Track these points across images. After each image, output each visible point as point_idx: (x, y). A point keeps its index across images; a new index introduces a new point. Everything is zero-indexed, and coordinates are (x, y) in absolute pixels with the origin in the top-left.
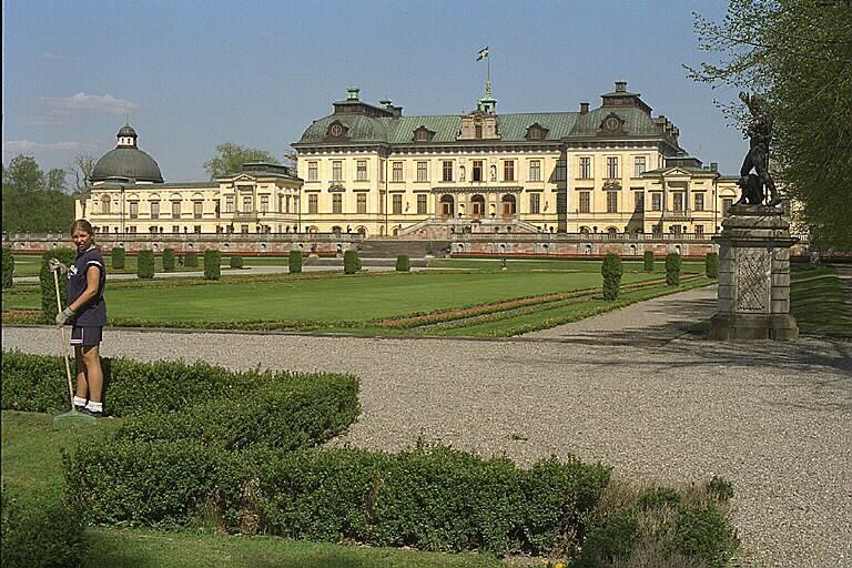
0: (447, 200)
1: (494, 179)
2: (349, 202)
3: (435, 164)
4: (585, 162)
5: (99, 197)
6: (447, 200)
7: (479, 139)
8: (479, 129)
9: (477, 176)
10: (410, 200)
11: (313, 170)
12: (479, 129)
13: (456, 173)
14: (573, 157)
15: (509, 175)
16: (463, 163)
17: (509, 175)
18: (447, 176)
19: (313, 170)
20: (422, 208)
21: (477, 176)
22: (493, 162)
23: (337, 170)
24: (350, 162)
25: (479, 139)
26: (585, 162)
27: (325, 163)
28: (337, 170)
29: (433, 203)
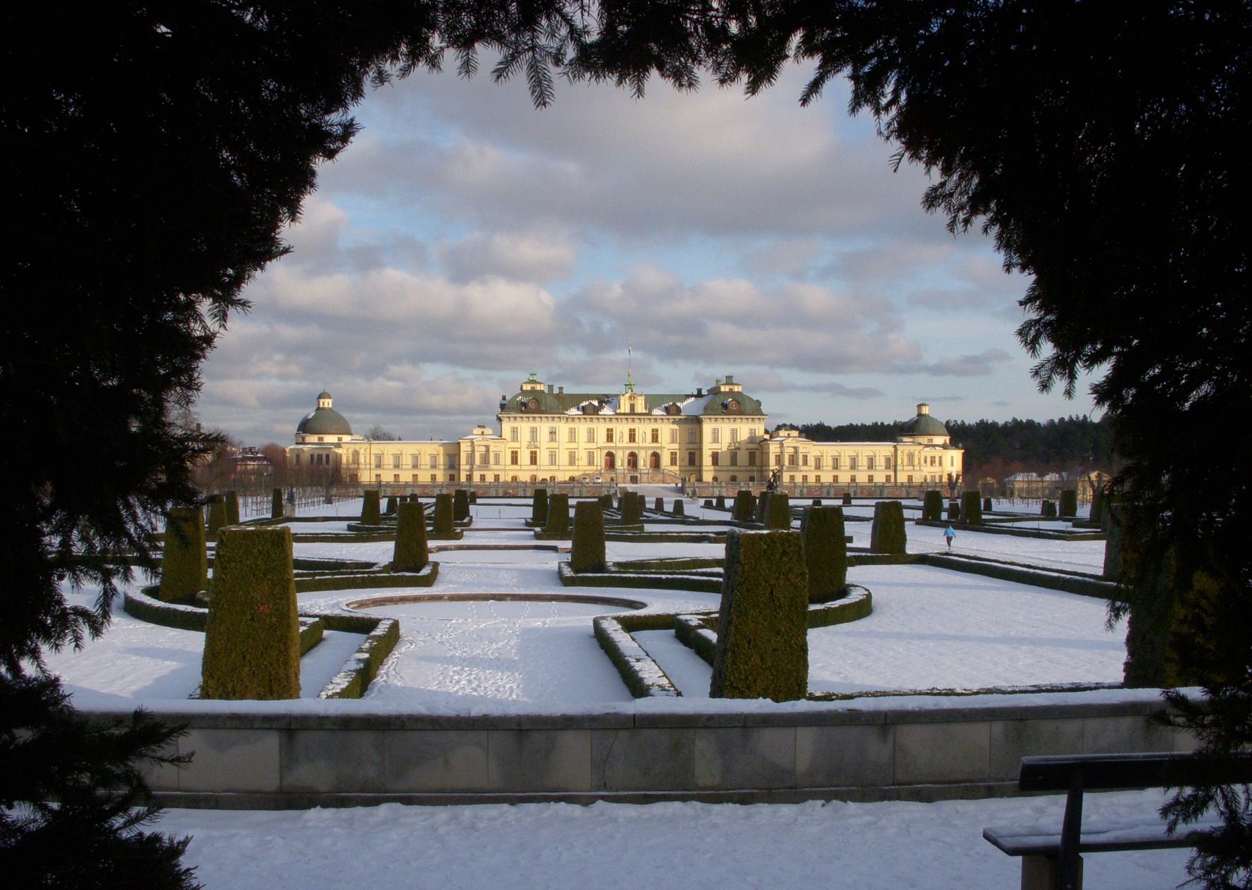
0: (611, 457)
1: (644, 440)
2: (543, 458)
3: (601, 429)
4: (715, 433)
5: (351, 451)
6: (611, 457)
7: (633, 412)
8: (632, 407)
9: (632, 438)
10: (582, 456)
11: (514, 431)
12: (632, 407)
13: (616, 437)
14: (708, 428)
15: (655, 438)
16: (621, 429)
17: (655, 438)
18: (610, 438)
19: (514, 431)
20: (591, 463)
21: (632, 438)
22: (644, 429)
23: (534, 431)
24: (544, 426)
25: (633, 412)
26: (715, 433)
27: (524, 426)
28: (534, 431)
29: (600, 460)
